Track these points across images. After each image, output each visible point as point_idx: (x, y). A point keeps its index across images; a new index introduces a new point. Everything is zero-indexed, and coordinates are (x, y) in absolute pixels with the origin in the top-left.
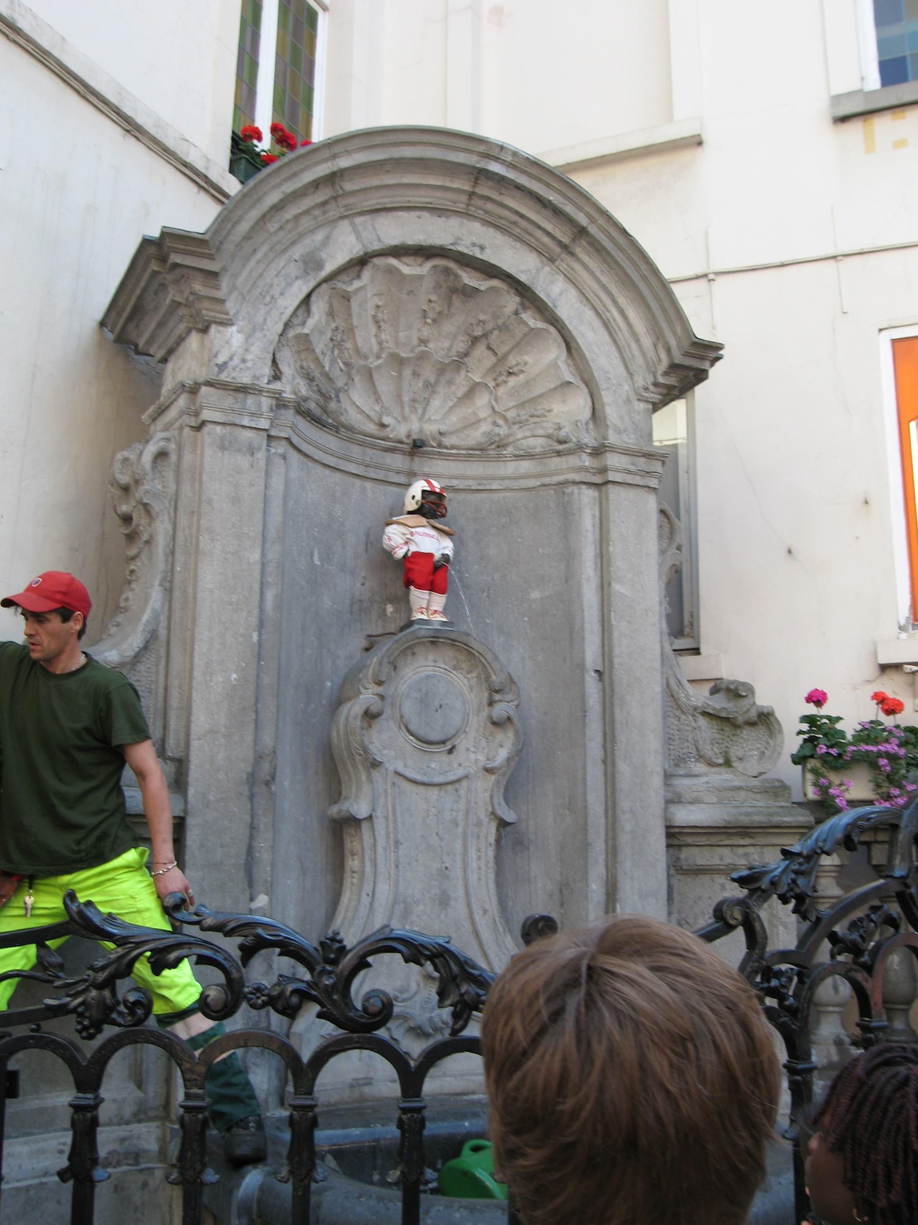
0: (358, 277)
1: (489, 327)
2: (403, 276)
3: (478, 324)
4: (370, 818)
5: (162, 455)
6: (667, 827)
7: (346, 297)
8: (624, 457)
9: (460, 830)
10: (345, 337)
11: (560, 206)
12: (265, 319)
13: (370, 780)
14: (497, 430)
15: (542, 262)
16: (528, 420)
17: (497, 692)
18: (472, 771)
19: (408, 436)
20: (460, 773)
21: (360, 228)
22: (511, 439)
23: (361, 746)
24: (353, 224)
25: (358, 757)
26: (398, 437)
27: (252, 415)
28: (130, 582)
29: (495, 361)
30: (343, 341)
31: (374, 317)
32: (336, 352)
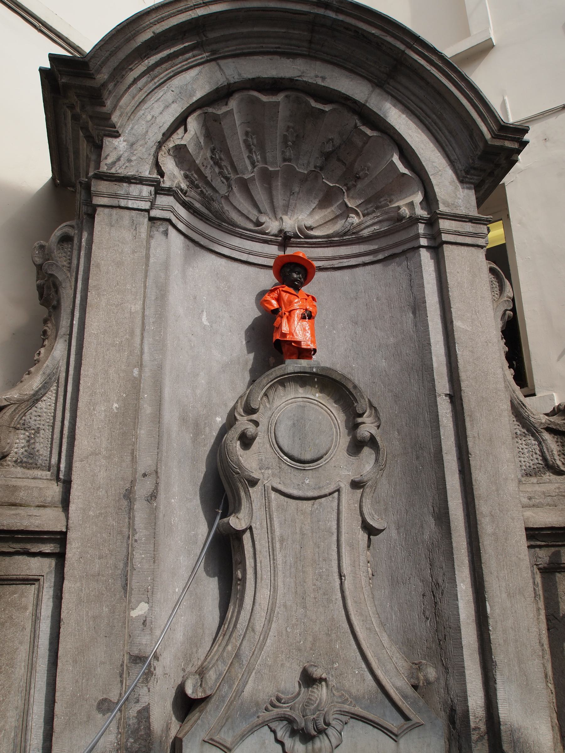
0: (226, 104)
1: (337, 142)
2: (264, 104)
6: (527, 529)
7: (217, 119)
8: (453, 222)
10: (222, 156)
11: (381, 36)
12: (147, 132)
13: (249, 496)
15: (372, 87)
16: (374, 212)
17: (361, 415)
18: (342, 485)
19: (281, 231)
20: (332, 488)
21: (222, 67)
22: (363, 226)
23: (238, 466)
24: (218, 64)
26: (272, 233)
27: (136, 198)
29: (344, 170)
30: (221, 159)
31: (245, 141)
32: (217, 170)
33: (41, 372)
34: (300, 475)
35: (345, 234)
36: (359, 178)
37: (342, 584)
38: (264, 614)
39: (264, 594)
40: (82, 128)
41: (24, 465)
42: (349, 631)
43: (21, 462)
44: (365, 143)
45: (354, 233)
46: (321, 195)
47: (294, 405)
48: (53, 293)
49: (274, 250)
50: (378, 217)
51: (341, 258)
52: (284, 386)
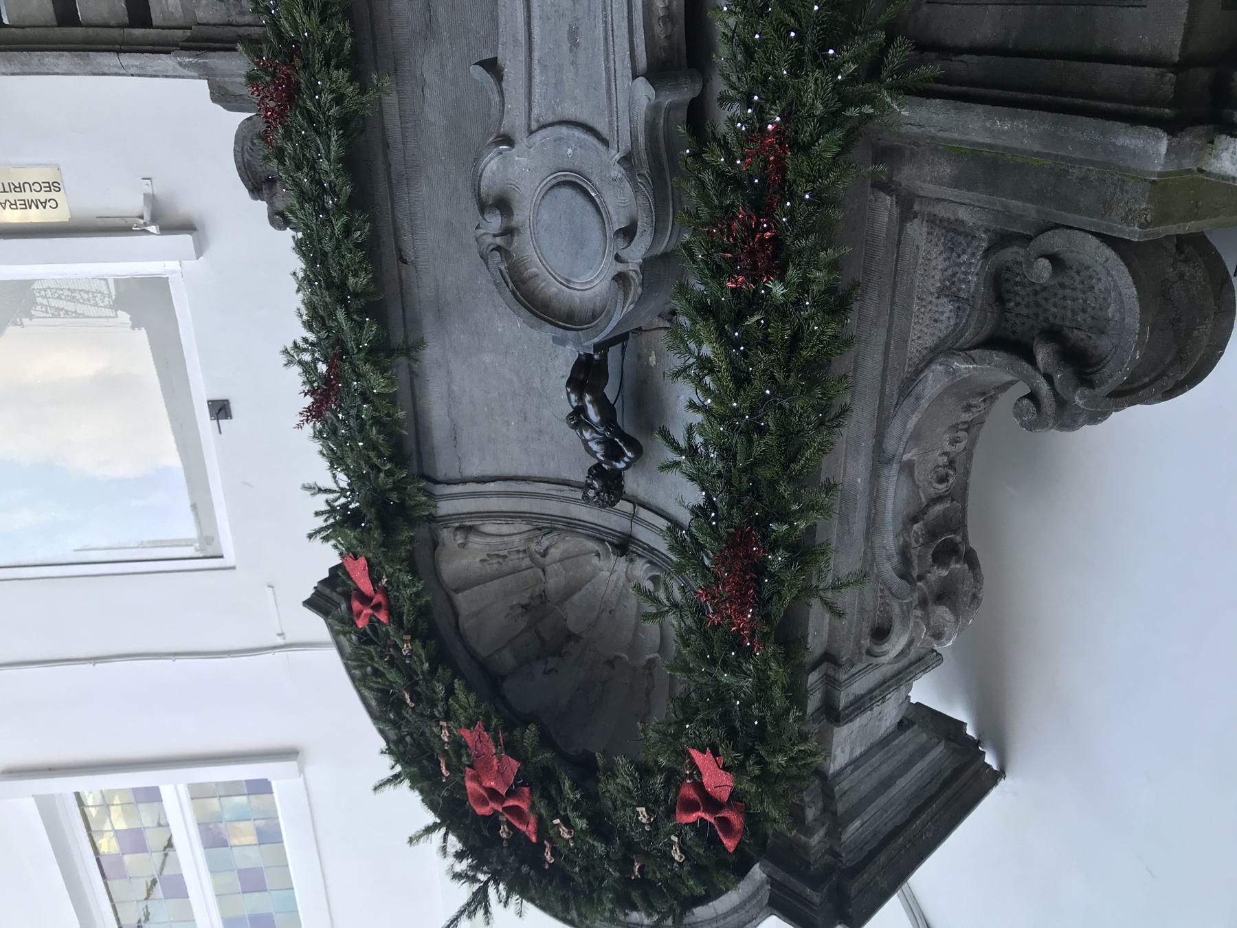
3: (551, 670)
4: (635, 76)
5: (881, 633)
9: (536, 55)
14: (541, 549)
19: (631, 561)
20: (538, 137)
22: (525, 536)
25: (645, 171)
26: (644, 561)
28: (951, 464)
33: (924, 403)
34: (577, 164)
36: (523, 607)
40: (835, 813)
41: (961, 229)
44: (499, 650)
45: (539, 529)
46: (576, 598)
47: (583, 279)
48: (914, 544)
49: (642, 534)
51: (556, 498)
52: (594, 311)
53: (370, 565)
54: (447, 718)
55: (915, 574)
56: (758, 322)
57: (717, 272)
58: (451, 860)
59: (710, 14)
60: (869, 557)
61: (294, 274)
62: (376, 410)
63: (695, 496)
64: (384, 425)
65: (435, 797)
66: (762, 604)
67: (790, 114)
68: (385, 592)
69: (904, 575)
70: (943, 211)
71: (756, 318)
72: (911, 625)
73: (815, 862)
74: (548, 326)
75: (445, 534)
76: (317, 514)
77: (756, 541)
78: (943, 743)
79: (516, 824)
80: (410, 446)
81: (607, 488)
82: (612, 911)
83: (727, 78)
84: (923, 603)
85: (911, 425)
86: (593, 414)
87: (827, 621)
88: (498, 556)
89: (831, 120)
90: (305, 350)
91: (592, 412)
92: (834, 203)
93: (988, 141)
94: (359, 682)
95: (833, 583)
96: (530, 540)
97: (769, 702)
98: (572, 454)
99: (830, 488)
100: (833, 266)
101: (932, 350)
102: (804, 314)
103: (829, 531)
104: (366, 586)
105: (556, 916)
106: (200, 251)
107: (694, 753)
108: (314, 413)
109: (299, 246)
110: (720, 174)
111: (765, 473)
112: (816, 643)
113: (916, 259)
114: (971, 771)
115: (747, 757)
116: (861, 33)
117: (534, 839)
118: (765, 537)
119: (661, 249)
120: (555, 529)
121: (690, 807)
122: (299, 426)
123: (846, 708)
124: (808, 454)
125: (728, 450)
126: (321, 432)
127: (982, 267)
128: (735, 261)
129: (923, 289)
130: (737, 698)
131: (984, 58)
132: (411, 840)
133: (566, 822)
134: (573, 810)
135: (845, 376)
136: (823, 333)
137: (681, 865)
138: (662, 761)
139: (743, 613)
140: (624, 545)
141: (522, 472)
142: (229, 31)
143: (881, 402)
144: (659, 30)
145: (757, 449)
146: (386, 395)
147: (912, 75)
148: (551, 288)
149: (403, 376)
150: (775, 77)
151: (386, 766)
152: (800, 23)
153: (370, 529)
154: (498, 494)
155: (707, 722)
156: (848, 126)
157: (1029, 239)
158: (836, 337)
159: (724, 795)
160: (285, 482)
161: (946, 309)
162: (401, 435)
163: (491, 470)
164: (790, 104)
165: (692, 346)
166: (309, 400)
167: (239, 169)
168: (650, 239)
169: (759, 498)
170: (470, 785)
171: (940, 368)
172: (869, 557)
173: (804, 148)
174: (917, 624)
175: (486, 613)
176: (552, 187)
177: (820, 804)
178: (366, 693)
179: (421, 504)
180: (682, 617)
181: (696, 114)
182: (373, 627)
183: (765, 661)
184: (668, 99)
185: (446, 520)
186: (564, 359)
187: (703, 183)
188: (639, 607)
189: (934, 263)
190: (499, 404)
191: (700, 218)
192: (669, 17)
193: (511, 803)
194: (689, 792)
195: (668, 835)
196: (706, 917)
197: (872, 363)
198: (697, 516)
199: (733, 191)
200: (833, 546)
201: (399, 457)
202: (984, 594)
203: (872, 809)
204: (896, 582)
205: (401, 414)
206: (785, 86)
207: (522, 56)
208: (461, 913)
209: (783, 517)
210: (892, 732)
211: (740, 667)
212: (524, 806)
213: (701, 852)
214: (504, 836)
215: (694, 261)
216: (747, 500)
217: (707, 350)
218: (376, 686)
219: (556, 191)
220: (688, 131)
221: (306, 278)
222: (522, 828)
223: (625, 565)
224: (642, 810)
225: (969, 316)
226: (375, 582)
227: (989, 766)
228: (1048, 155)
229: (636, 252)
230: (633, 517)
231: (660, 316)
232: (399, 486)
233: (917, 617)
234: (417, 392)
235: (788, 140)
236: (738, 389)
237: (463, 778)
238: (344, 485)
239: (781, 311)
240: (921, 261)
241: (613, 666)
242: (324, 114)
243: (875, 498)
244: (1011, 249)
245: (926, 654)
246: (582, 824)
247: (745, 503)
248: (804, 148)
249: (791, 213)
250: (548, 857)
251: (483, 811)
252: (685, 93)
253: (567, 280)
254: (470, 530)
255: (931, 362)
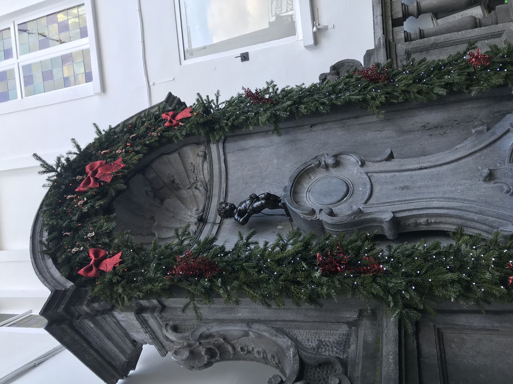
3: (148, 194)
4: (393, 212)
5: (175, 329)
9: (397, 174)
14: (198, 186)
17: (320, 163)
19: (196, 224)
20: (365, 176)
25: (356, 219)
26: (196, 229)
28: (249, 352)
33: (274, 338)
35: (207, 191)
36: (174, 181)
37: (426, 168)
38: (450, 203)
39: (435, 204)
40: (96, 315)
41: (347, 347)
42: (456, 163)
43: (344, 349)
44: (155, 172)
46: (179, 202)
47: (311, 197)
48: (214, 340)
49: (207, 227)
50: (200, 171)
51: (220, 192)
53: (188, 118)
54: (127, 152)
55: (202, 341)
56: (304, 267)
57: (322, 249)
58: (66, 156)
59: (423, 239)
60: (207, 321)
61: (303, 84)
62: (252, 118)
63: (229, 247)
64: (246, 121)
65: (92, 148)
66: (186, 277)
67: (387, 273)
68: (177, 125)
69: (201, 337)
70: (353, 339)
71: (305, 266)
72: (180, 341)
73: (75, 309)
74: (291, 184)
75: (202, 148)
76: (208, 96)
77: (210, 274)
78: (127, 360)
79: (83, 182)
80: (238, 132)
81: (226, 211)
82: (48, 224)
83: (398, 248)
84: (189, 346)
85: (265, 334)
86: (258, 203)
87: (179, 306)
88: (194, 169)
89: (387, 290)
90: (273, 89)
91: (258, 203)
92: (354, 294)
93: (384, 354)
94: (139, 116)
95: (196, 307)
96: (202, 182)
97: (145, 284)
98: (238, 197)
99: (237, 302)
100: (329, 296)
101: (296, 339)
102: (308, 286)
103: (219, 304)
104: (179, 117)
105: (44, 201)
106: (307, 47)
107: (120, 254)
108: (249, 93)
109: (315, 85)
110: (360, 248)
111: (242, 275)
112: (170, 302)
113: (332, 330)
114: (115, 374)
115: (120, 276)
116: (421, 299)
117: (76, 190)
118: (214, 277)
119: (326, 227)
120: (207, 192)
121: (96, 254)
122: (243, 88)
123: (142, 317)
124: (251, 292)
125: (250, 259)
126: (241, 97)
127: (333, 357)
128: (327, 256)
129: (320, 333)
130: (145, 270)
131: (416, 349)
132: (73, 139)
133: (85, 203)
134: (91, 205)
135: (284, 305)
136: (301, 294)
137: (70, 252)
138: (116, 241)
139: (182, 270)
140: (202, 220)
141: (229, 177)
142: (394, 56)
143: (274, 321)
144: (412, 221)
145: (251, 271)
146: (258, 122)
147: (407, 321)
148: (306, 185)
149: (266, 128)
150: (401, 267)
151: (104, 127)
152: (422, 275)
153: (203, 118)
154: (220, 168)
155: (133, 259)
156: (385, 297)
157: (346, 373)
158: (299, 300)
159: (102, 268)
160: (221, 83)
161: (314, 344)
162: (242, 128)
163: (230, 165)
164: (391, 273)
165: (291, 241)
166: (254, 92)
167: (342, 61)
168: (330, 222)
169: (231, 273)
170: (98, 163)
171: (290, 343)
172: (207, 321)
173: (374, 281)
174: (180, 344)
175: (170, 165)
176: (346, 183)
177: (100, 309)
178: (134, 119)
179: (214, 137)
180: (177, 245)
181: (380, 238)
182: (162, 120)
183: (162, 281)
184: (386, 226)
185: (208, 147)
186: (278, 192)
187: (356, 241)
188: (181, 228)
189: (331, 337)
190: (257, 167)
191: (342, 241)
192: (417, 224)
193: (92, 180)
194: (102, 253)
195: (83, 246)
196: (47, 264)
197: (289, 316)
198: (221, 248)
199: (354, 254)
200: (213, 306)
201: (234, 128)
202: (194, 371)
203: (99, 332)
204: (198, 334)
205: (251, 128)
206: (398, 271)
207: (396, 168)
208: (43, 161)
209: (224, 283)
210: (131, 338)
211: (158, 271)
212: (91, 185)
213: (77, 260)
214: (77, 178)
215: (325, 240)
216: (230, 268)
217: (290, 248)
218: (137, 123)
219: (345, 184)
220: (375, 234)
221: (302, 89)
222: (81, 185)
223: (194, 221)
224: (93, 234)
225: (312, 353)
226: (181, 120)
227: (117, 382)
228: (381, 379)
229: (324, 217)
230: (214, 223)
231: (298, 228)
232: (221, 128)
233: (184, 343)
234: (259, 134)
235: (377, 274)
236: (274, 261)
237: (101, 159)
238: (220, 106)
239: (308, 276)
240: (332, 332)
241: (151, 219)
242: (367, 93)
243: (233, 321)
244: (341, 368)
245: (165, 350)
246: (85, 209)
247: (228, 267)
248: (374, 281)
249: (348, 277)
250: (69, 196)
251: (87, 168)
252: (388, 233)
253: (309, 191)
254: (205, 157)
255: (292, 339)
